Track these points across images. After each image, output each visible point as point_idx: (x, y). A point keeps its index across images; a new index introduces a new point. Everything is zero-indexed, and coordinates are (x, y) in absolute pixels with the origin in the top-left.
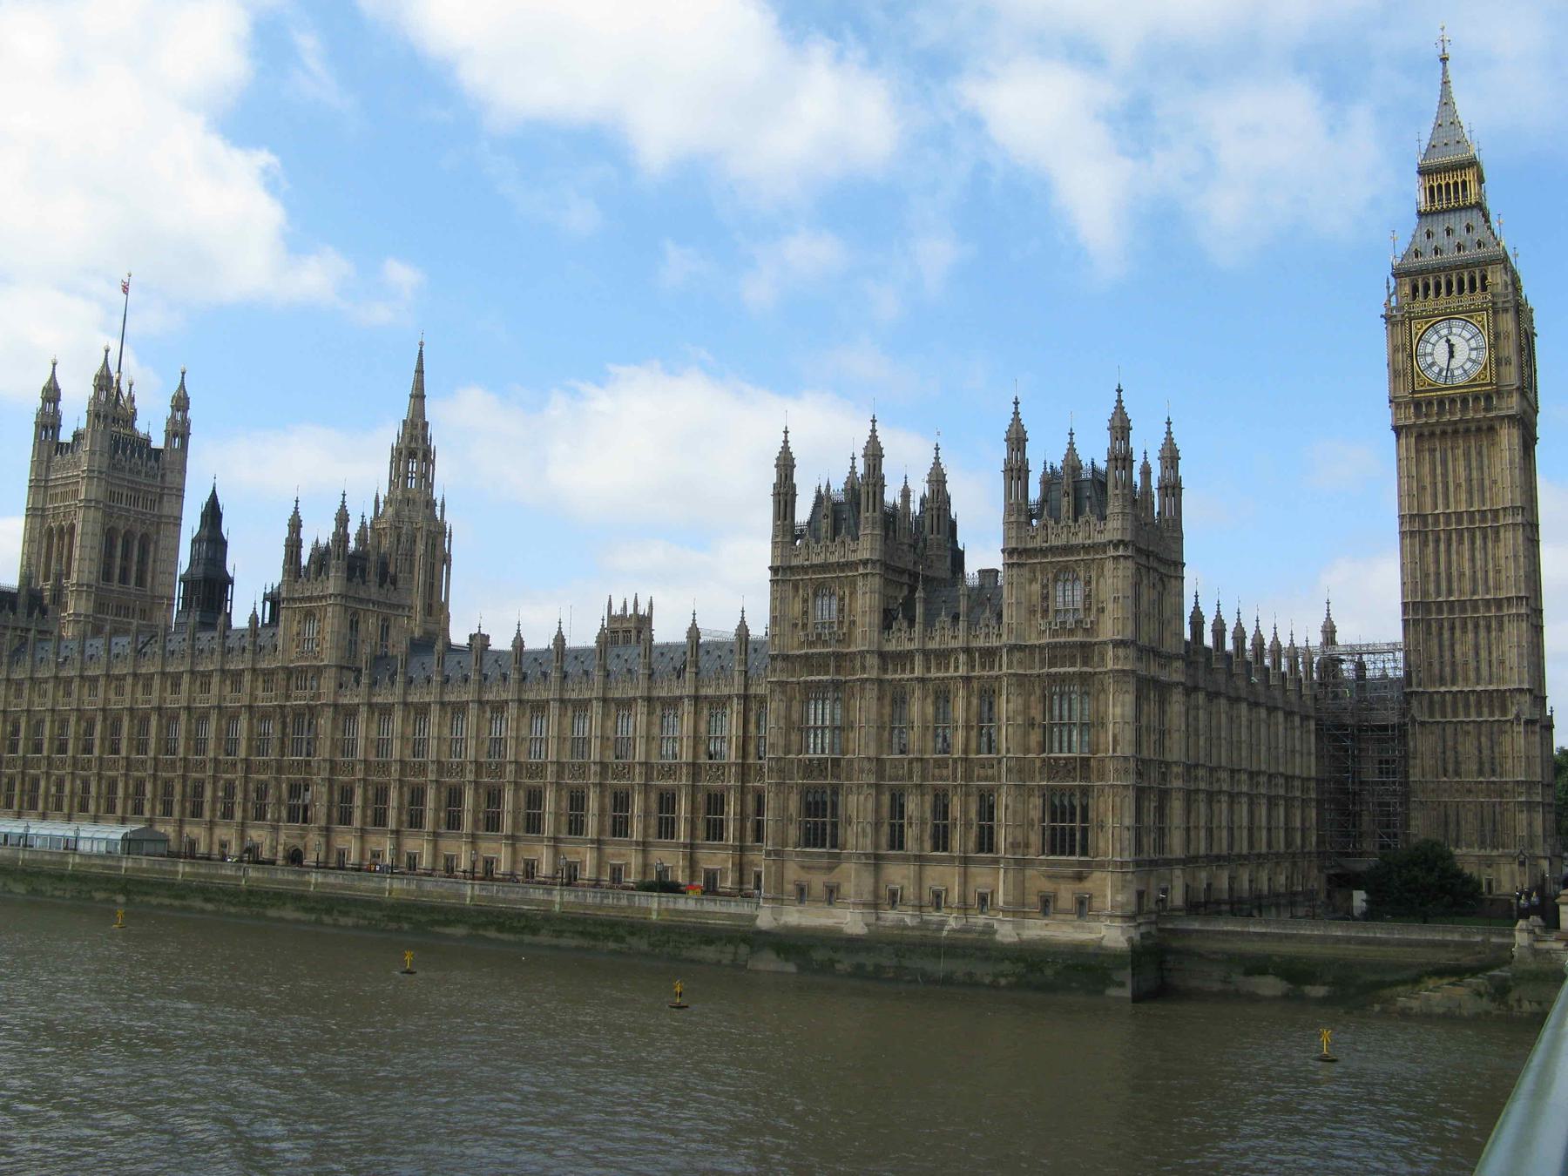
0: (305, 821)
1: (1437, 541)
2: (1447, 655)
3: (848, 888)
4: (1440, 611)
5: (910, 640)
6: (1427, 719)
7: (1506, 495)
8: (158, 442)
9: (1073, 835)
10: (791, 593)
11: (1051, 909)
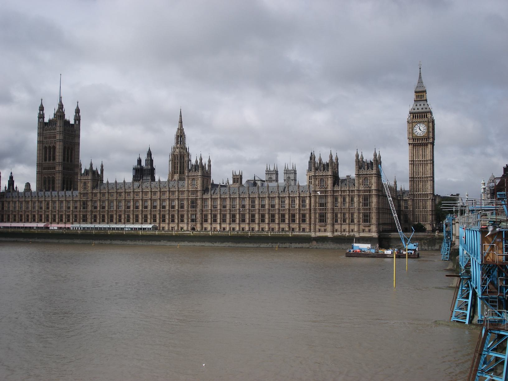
7: (429, 157)
8: (72, 122)
9: (368, 220)
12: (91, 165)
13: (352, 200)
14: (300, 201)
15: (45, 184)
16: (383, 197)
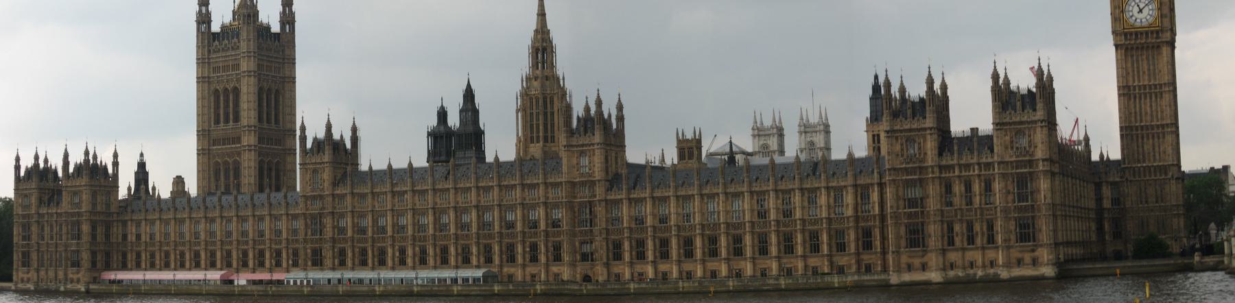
0: (592, 260)
1: (1135, 97)
2: (1141, 150)
3: (930, 264)
4: (1137, 130)
5: (952, 160)
6: (1132, 178)
8: (276, 28)
9: (1029, 235)
10: (894, 141)
11: (1022, 262)
12: (329, 127)
13: (988, 188)
14: (857, 197)
15: (217, 180)
16: (1061, 176)
